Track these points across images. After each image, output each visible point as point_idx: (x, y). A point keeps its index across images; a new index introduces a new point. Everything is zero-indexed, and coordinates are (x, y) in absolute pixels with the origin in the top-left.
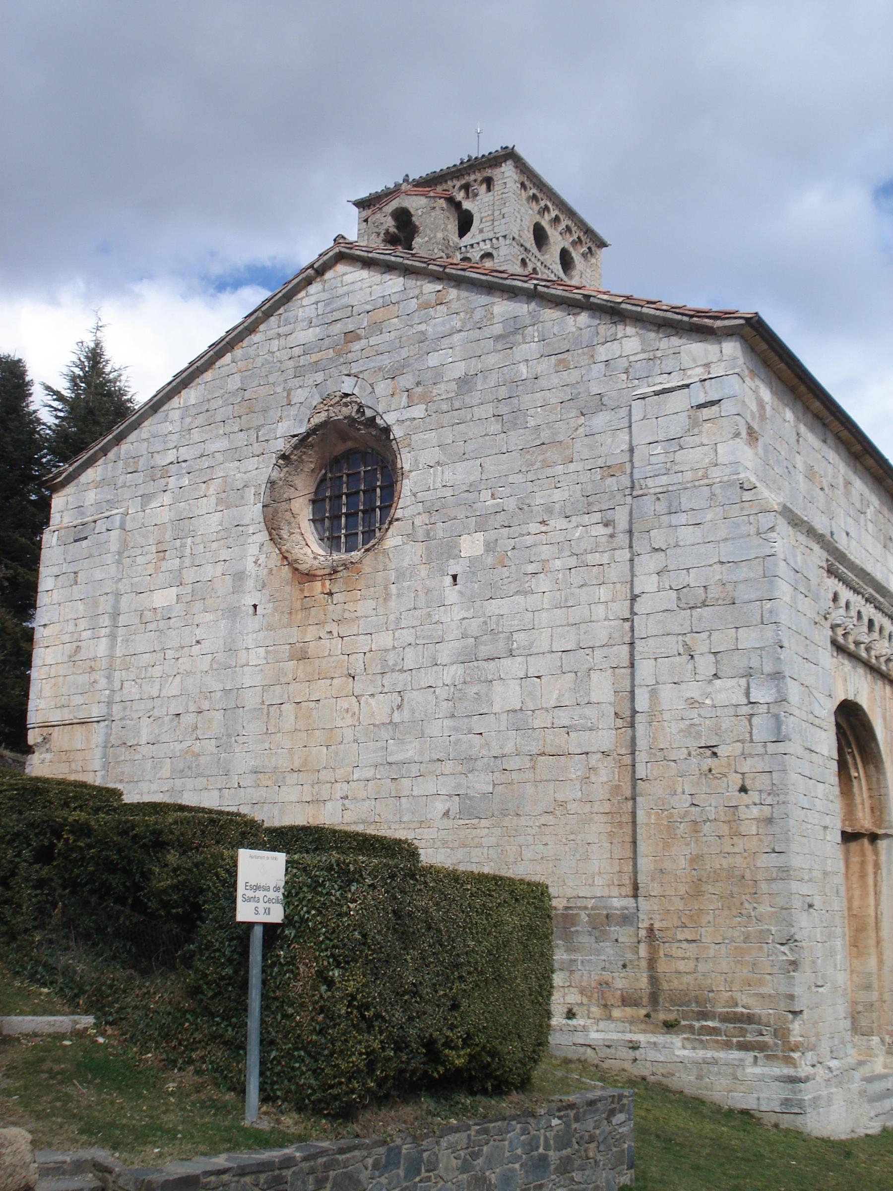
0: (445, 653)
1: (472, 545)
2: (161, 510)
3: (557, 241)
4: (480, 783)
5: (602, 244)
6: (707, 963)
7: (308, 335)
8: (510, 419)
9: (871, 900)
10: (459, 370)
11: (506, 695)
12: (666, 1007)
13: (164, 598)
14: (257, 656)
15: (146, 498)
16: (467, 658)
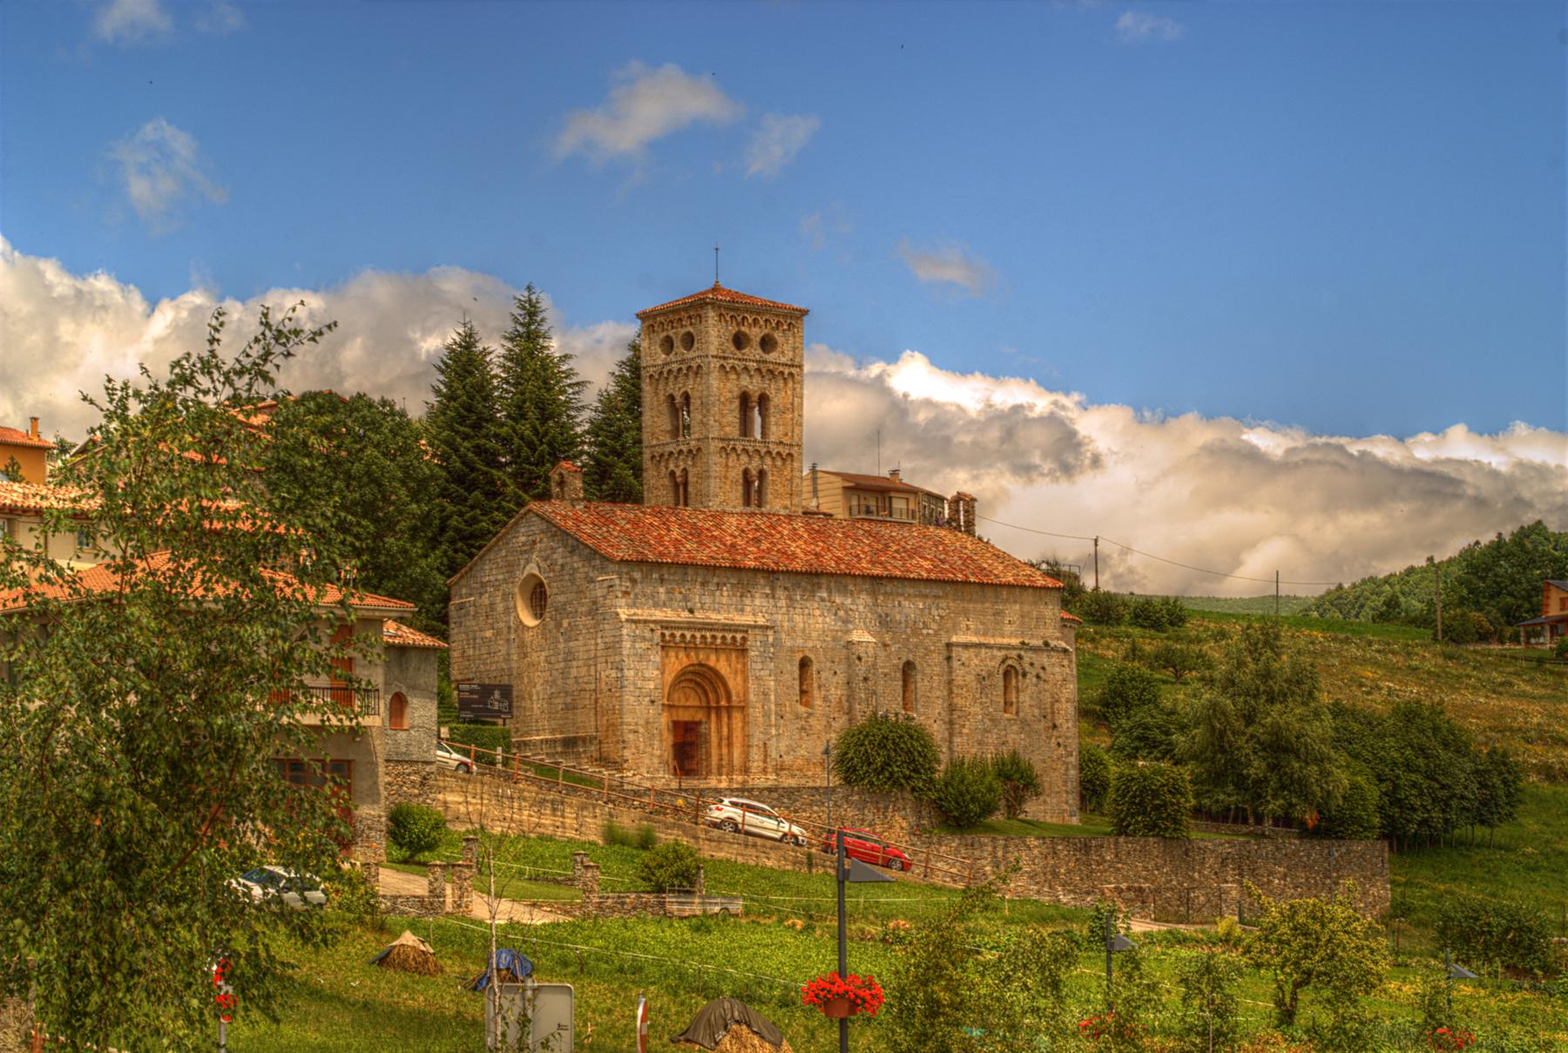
0: (561, 657)
1: (565, 623)
2: (485, 600)
3: (756, 333)
4: (569, 700)
5: (804, 312)
6: (609, 748)
7: (523, 539)
8: (573, 581)
9: (725, 730)
10: (560, 562)
11: (574, 672)
12: (603, 760)
13: (489, 634)
14: (515, 657)
15: (481, 594)
16: (565, 660)
